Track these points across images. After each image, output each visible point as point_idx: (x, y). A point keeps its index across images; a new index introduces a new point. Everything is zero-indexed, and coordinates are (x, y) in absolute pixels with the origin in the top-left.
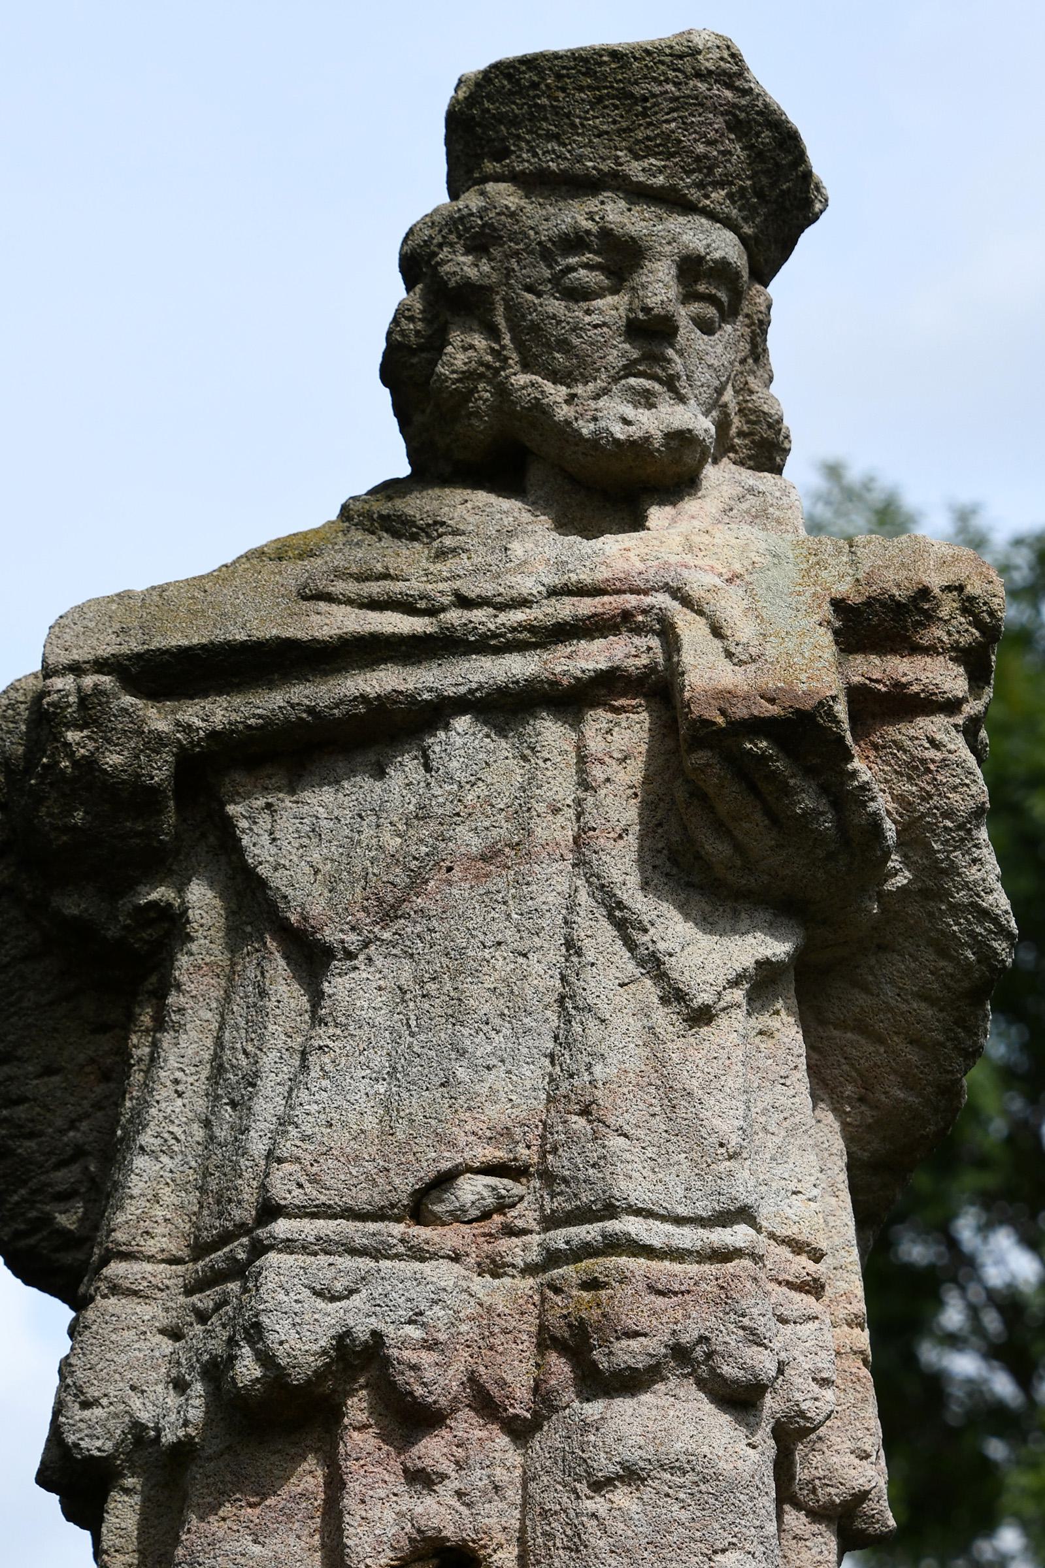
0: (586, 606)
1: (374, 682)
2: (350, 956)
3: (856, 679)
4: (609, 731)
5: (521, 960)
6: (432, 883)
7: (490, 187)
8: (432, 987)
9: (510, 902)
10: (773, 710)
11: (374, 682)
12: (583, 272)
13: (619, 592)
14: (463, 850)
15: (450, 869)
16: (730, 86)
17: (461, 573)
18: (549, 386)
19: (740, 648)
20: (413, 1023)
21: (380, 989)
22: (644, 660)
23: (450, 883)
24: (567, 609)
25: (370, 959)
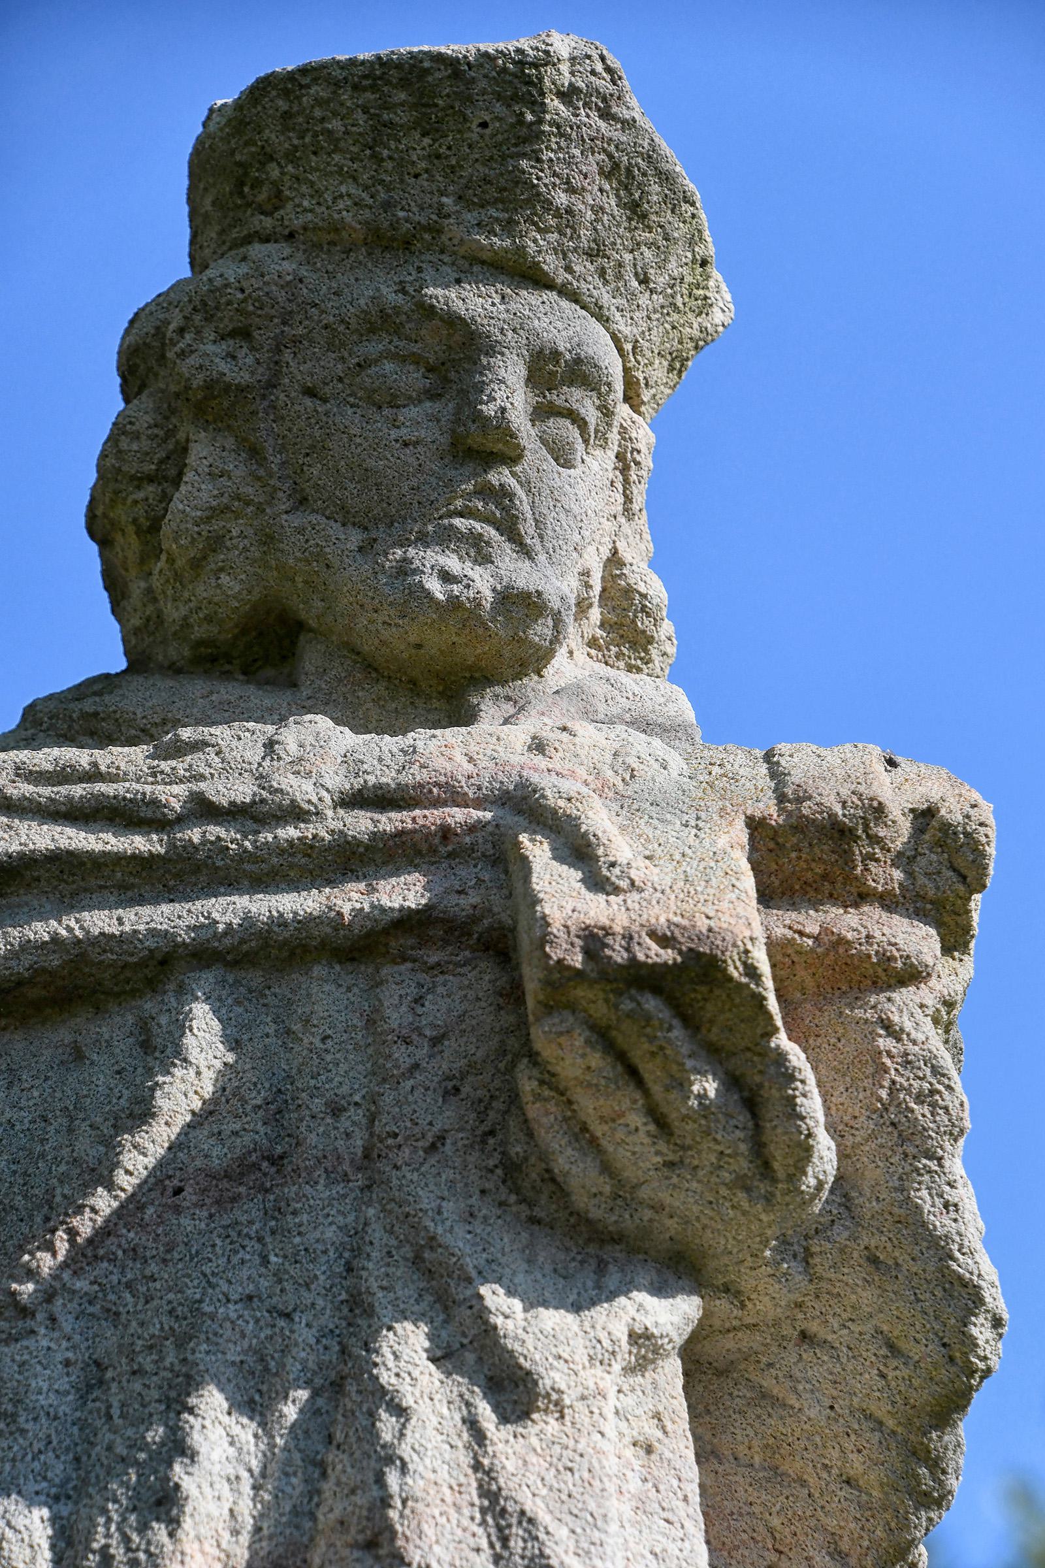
0: (390, 821)
1: (72, 923)
2: (24, 1312)
3: (780, 931)
4: (419, 1000)
5: (281, 1323)
6: (150, 1211)
7: (257, 250)
8: (147, 1361)
9: (268, 1240)
10: (668, 956)
11: (72, 923)
12: (388, 366)
13: (437, 803)
14: (198, 1163)
15: (178, 1191)
16: (606, 115)
17: (207, 771)
18: (335, 529)
19: (617, 871)
20: (115, 1412)
21: (67, 1363)
22: (473, 898)
23: (177, 1210)
24: (361, 823)
25: (53, 1319)
